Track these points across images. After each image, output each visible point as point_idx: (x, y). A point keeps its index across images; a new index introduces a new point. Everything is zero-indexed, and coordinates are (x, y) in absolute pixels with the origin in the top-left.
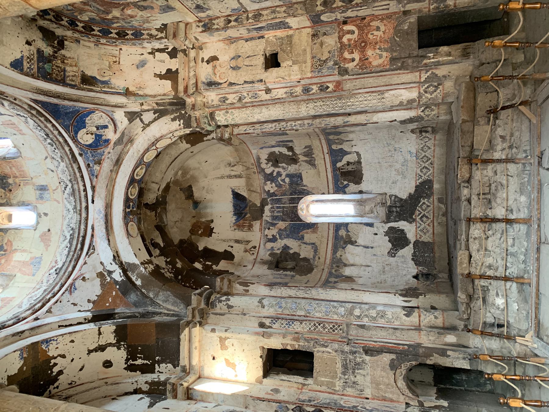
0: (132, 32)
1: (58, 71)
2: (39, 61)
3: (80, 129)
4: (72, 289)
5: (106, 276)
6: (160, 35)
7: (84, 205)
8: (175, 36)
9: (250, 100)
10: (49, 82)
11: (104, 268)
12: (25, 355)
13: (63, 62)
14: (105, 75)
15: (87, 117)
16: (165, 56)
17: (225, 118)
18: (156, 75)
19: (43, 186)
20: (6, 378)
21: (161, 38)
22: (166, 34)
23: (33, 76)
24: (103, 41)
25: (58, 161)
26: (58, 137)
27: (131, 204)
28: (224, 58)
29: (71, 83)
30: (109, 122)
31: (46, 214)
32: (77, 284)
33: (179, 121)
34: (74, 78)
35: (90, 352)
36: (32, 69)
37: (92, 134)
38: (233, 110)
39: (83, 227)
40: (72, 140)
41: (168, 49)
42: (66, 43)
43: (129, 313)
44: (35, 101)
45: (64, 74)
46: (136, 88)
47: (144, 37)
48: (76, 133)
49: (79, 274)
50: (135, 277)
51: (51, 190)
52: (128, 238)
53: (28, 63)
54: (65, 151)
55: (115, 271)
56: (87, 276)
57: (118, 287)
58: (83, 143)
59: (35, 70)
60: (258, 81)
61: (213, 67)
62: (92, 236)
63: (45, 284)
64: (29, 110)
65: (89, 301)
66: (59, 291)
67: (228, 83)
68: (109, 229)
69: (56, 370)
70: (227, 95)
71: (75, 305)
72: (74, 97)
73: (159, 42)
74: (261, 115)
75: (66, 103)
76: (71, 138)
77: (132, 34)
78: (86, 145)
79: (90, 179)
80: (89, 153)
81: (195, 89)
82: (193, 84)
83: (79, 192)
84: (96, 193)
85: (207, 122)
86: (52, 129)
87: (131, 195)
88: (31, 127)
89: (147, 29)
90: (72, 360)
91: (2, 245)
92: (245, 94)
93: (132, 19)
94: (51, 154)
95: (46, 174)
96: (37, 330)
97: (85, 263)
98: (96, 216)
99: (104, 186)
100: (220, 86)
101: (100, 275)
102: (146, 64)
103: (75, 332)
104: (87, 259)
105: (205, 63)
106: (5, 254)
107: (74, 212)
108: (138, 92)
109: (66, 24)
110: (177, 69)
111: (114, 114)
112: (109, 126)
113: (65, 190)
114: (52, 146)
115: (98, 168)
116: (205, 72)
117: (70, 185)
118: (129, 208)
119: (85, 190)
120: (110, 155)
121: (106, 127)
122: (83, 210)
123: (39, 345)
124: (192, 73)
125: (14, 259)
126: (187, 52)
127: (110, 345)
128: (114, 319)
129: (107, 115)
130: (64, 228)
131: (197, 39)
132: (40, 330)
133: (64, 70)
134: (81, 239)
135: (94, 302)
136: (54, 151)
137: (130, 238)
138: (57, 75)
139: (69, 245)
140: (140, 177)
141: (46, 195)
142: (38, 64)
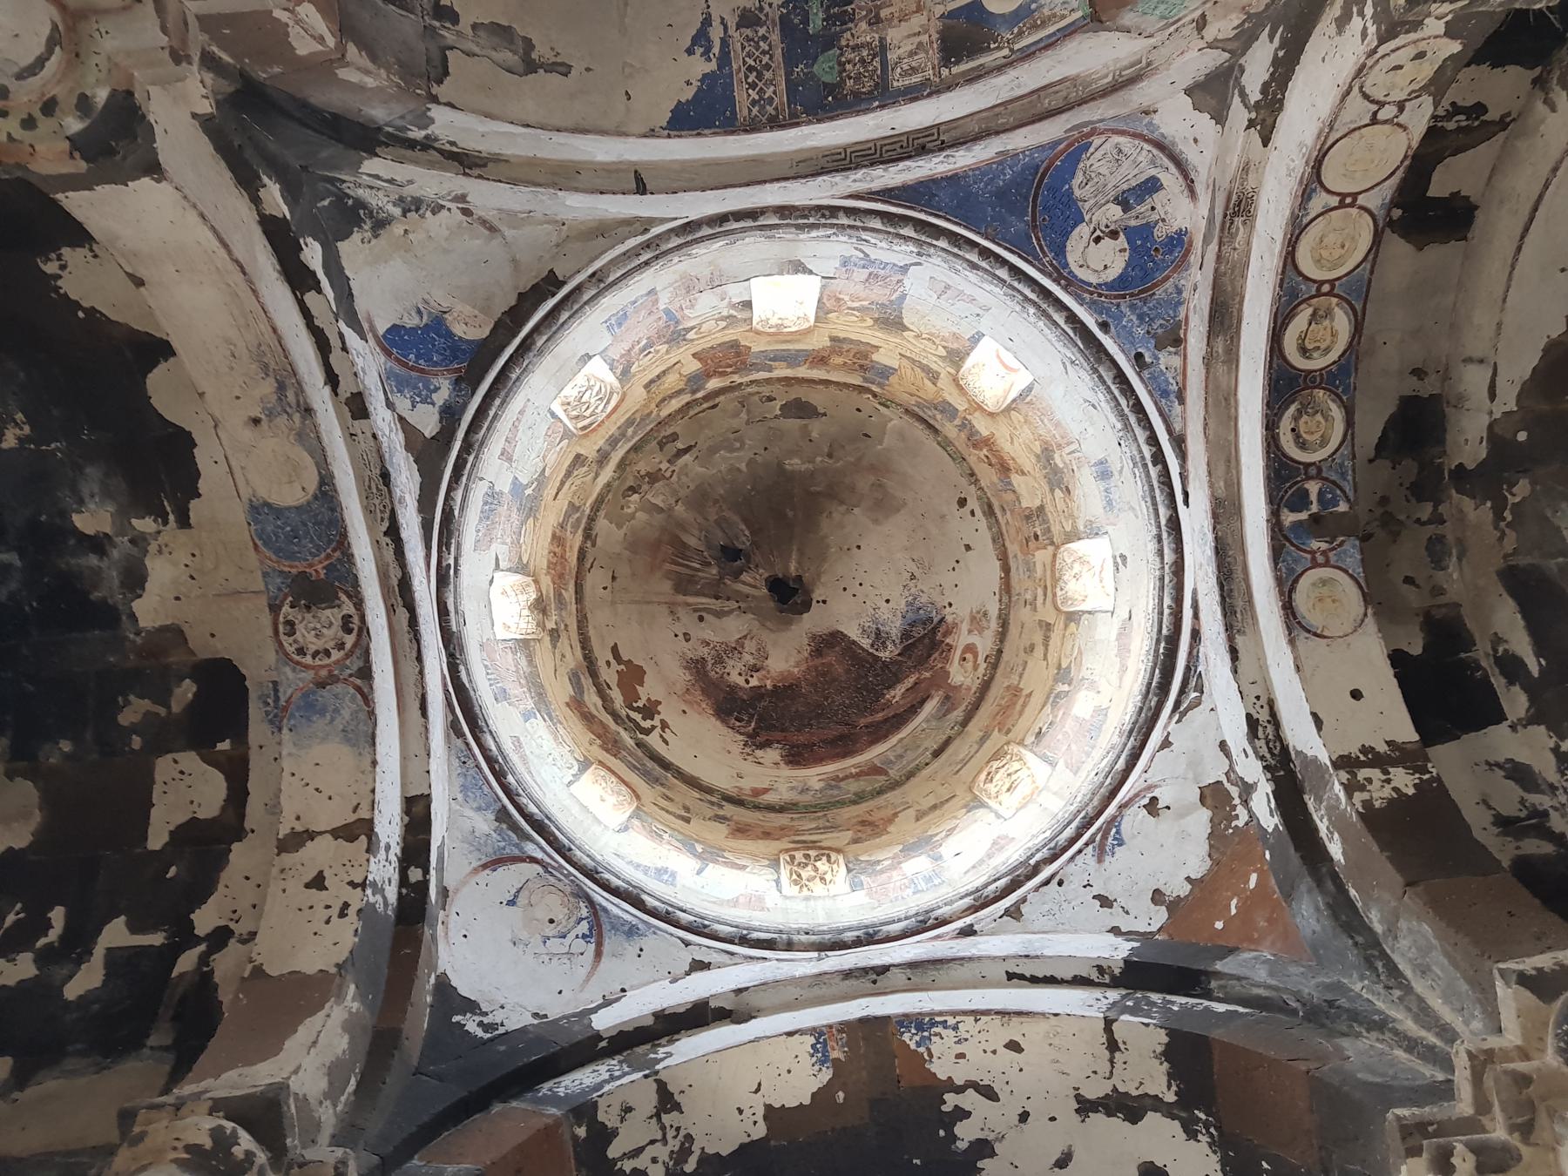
2: (790, 60)
3: (1066, 235)
5: (1237, 801)
10: (832, 119)
11: (1231, 768)
12: (835, 1054)
13: (875, 21)
20: (761, 1111)
23: (775, 123)
27: (1313, 488)
29: (907, 82)
30: (1153, 163)
32: (1126, 826)
35: (1085, 1107)
37: (1114, 235)
39: (1167, 601)
43: (1258, 986)
44: (886, 194)
45: (884, 63)
48: (1060, 251)
49: (1141, 785)
52: (1292, 642)
53: (753, 86)
56: (1165, 796)
58: (1093, 279)
62: (1196, 635)
65: (1157, 897)
68: (1239, 604)
69: (966, 1133)
71: (1105, 902)
76: (1049, 275)
78: (1110, 286)
79: (1161, 414)
87: (1302, 445)
90: (1024, 1117)
96: (932, 974)
101: (1214, 796)
103: (1019, 1013)
112: (1165, 178)
115: (1176, 361)
118: (1301, 501)
119: (1159, 458)
121: (1152, 186)
123: (891, 1029)
127: (1156, 1103)
128: (1208, 995)
129: (1135, 136)
132: (941, 975)
133: (883, 48)
135: (1174, 906)
137: (1306, 643)
138: (858, 77)
140: (1333, 356)
142: (788, 74)
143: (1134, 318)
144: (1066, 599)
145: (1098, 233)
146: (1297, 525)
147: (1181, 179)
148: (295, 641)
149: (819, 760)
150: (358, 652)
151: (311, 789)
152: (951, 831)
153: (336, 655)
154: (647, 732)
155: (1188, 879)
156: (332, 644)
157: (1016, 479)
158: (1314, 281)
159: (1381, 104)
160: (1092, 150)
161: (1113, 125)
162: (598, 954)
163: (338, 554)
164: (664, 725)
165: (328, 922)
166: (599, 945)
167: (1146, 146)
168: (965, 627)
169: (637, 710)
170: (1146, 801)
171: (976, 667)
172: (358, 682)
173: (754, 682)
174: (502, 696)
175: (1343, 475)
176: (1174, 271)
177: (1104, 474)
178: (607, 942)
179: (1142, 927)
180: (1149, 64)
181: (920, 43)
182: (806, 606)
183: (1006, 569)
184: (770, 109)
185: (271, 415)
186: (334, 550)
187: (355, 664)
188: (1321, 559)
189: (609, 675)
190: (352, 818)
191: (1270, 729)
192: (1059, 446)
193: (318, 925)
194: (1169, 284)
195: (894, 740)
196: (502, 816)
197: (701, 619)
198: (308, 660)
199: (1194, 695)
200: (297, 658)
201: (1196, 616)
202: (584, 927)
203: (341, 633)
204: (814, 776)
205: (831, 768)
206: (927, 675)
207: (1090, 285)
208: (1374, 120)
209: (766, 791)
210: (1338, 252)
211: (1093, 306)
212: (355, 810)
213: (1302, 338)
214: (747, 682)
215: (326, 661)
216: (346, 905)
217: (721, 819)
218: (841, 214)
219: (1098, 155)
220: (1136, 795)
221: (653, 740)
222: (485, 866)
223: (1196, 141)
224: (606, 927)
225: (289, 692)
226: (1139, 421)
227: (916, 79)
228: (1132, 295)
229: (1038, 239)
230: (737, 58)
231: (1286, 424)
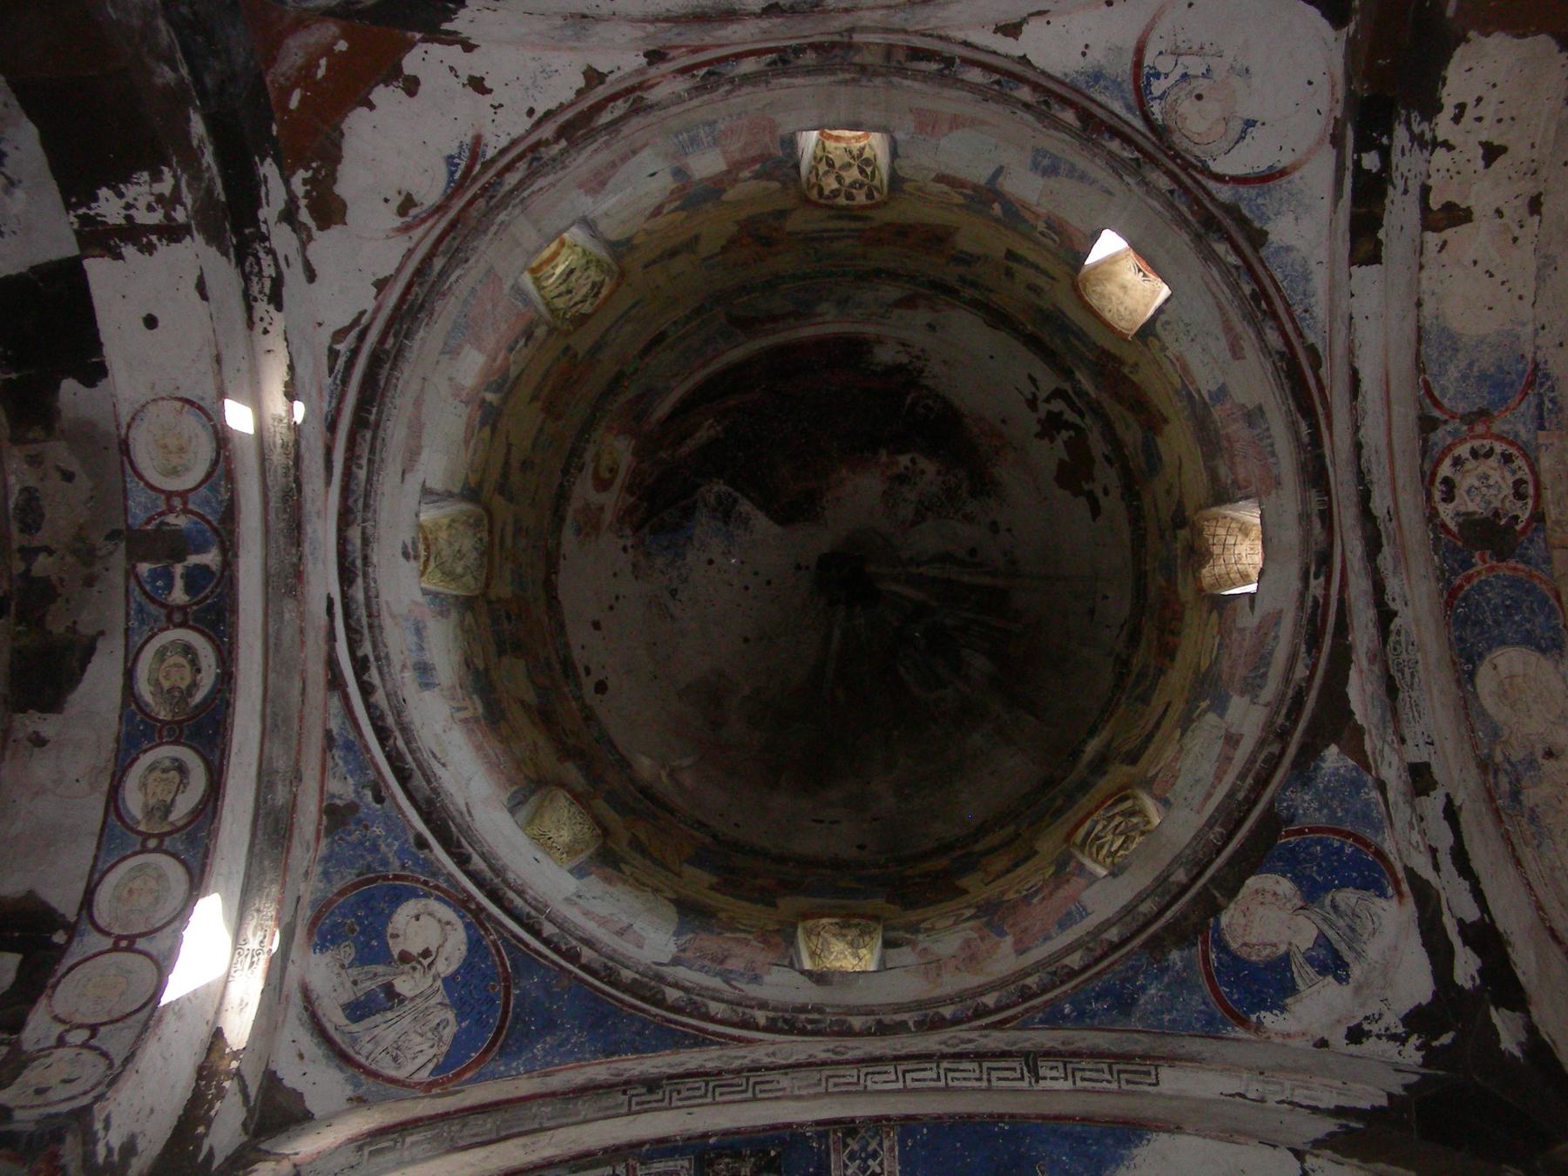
3: (468, 966)
5: (303, 203)
10: (774, 1127)
11: (304, 246)
15: (456, 1037)
23: (849, 1127)
27: (179, 595)
30: (354, 1040)
36: (852, 1157)
37: (405, 957)
48: (475, 945)
49: (418, 233)
65: (412, 86)
71: (477, 85)
72: (584, 1108)
75: (599, 1071)
76: (490, 917)
78: (414, 894)
87: (188, 650)
101: (329, 211)
104: (370, 305)
111: (349, 1091)
115: (334, 786)
118: (197, 577)
119: (360, 666)
121: (358, 1010)
129: (375, 1075)
135: (393, 74)
140: (146, 760)
144: (476, 525)
145: (426, 962)
146: (201, 549)
147: (320, 1013)
148: (1514, 472)
149: (821, 343)
150: (1436, 452)
151: (1499, 277)
152: (657, 211)
154: (1058, 394)
156: (1468, 466)
157: (531, 697)
158: (167, 852)
159: (84, 1045)
160: (431, 1066)
162: (1140, 51)
163: (1457, 581)
164: (1032, 403)
165: (1479, 100)
166: (1138, 64)
167: (362, 1060)
168: (608, 516)
169: (1069, 426)
170: (413, 212)
171: (597, 457)
172: (1436, 413)
173: (904, 460)
174: (1253, 416)
175: (141, 610)
176: (330, 902)
177: (424, 669)
178: (1128, 66)
179: (437, 50)
180: (360, 1148)
182: (825, 562)
183: (550, 586)
184: (854, 1145)
185: (1531, 763)
186: (1461, 587)
187: (1440, 436)
188: (177, 502)
189: (1106, 476)
190: (1448, 233)
191: (255, 289)
193: (1492, 97)
194: (338, 885)
195: (715, 366)
196: (1258, 238)
197: (973, 552)
198: (1499, 447)
199: (341, 347)
201: (329, 451)
202: (1158, 87)
203: (1457, 478)
204: (829, 323)
205: (807, 332)
206: (663, 455)
207: (438, 898)
208: (94, 1029)
209: (899, 304)
210: (138, 884)
211: (434, 870)
212: (1445, 243)
214: (913, 461)
215: (1476, 443)
216: (1457, 119)
217: (966, 259)
219: (421, 1060)
220: (423, 221)
221: (1048, 381)
222: (1283, 173)
223: (301, 1056)
224: (1129, 86)
225: (1524, 405)
226: (382, 717)
228: (386, 878)
229: (503, 964)
231: (207, 679)
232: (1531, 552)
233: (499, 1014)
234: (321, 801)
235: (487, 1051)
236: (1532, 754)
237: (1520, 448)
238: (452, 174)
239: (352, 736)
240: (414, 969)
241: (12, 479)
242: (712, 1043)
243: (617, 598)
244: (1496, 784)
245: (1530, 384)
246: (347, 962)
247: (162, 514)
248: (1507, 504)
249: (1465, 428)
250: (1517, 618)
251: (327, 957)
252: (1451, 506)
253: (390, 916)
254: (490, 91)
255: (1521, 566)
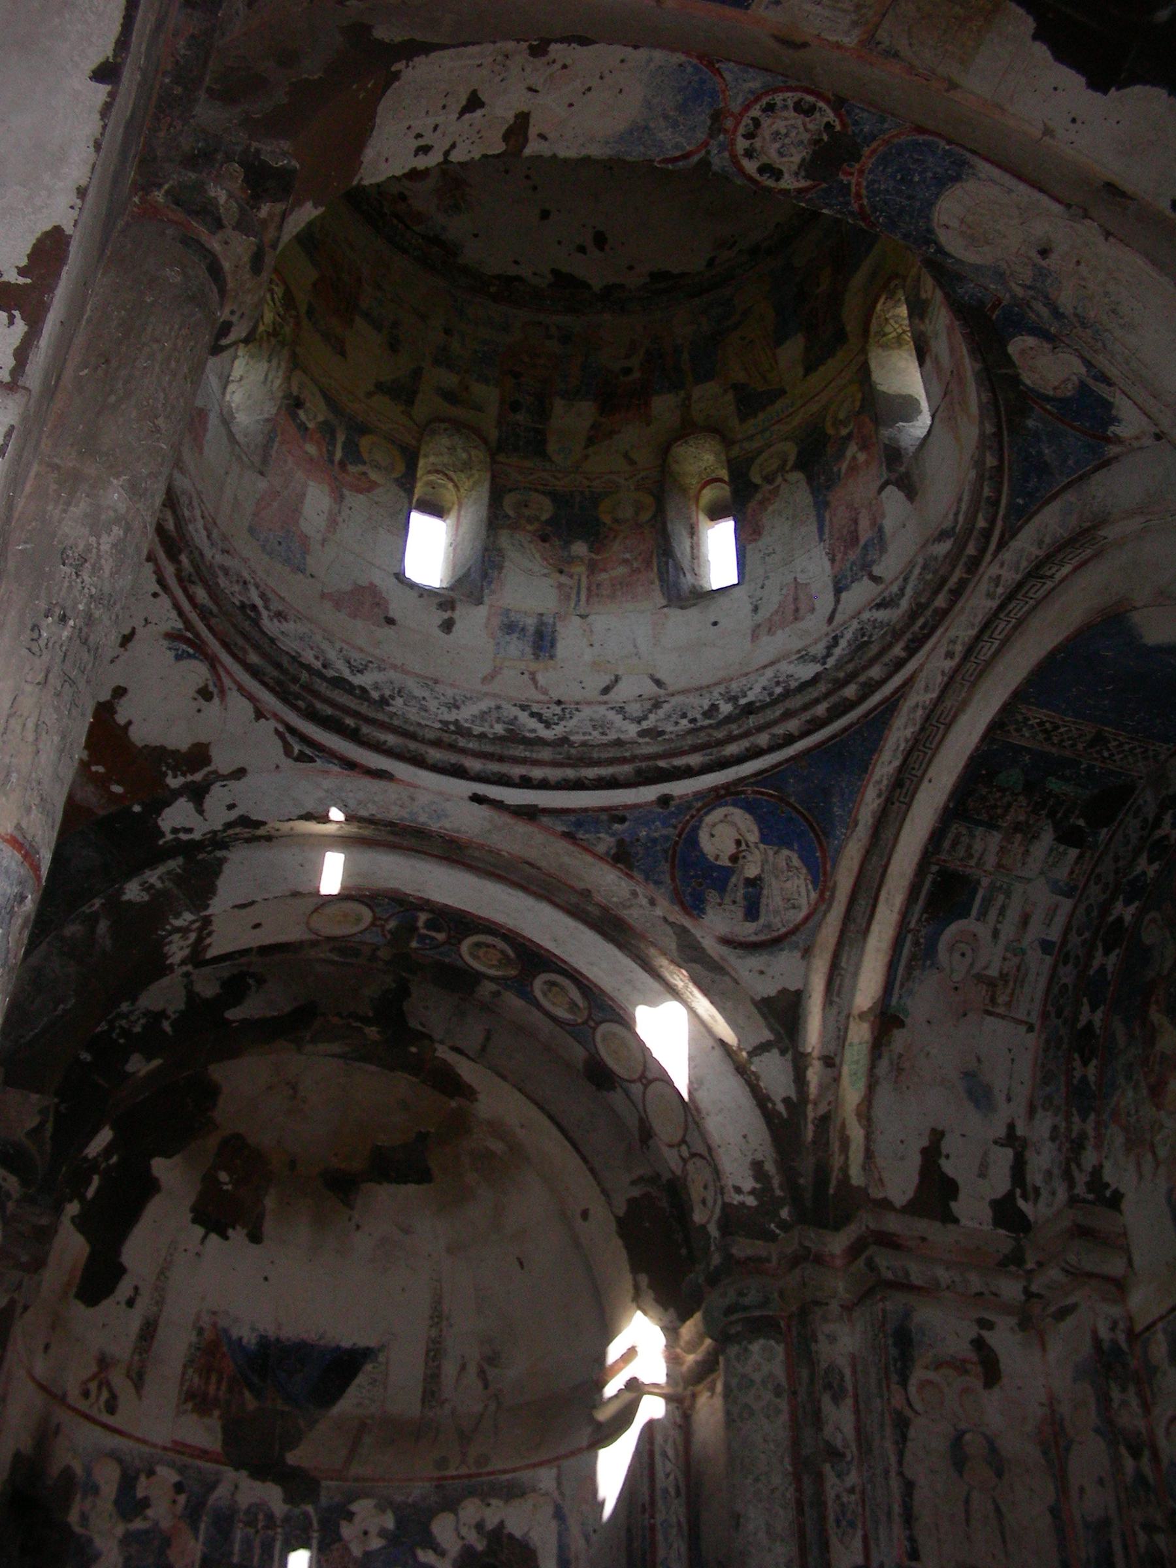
0: (1092, 1079)
1: (995, 807)
3: (760, 820)
4: (185, 642)
5: (190, 778)
6: (1081, 1179)
7: (474, 765)
8: (1082, 1232)
9: (831, 1494)
13: (1017, 828)
14: (957, 955)
15: (801, 858)
16: (999, 1183)
17: (757, 1377)
18: (937, 1136)
19: (553, 644)
21: (1071, 1184)
22: (1084, 1201)
23: (996, 727)
24: (1067, 975)
25: (645, 718)
26: (745, 744)
27: (441, 937)
28: (992, 1410)
29: (950, 836)
30: (768, 926)
31: (448, 626)
33: (753, 1192)
34: (961, 852)
37: (734, 858)
38: (784, 1417)
39: (391, 739)
40: (726, 786)
41: (1025, 1197)
42: (1073, 853)
44: (891, 706)
45: (979, 823)
46: (900, 1056)
47: (1076, 1119)
48: (749, 807)
49: (227, 682)
50: (159, 885)
51: (533, 666)
53: (1041, 724)
54: (683, 753)
55: (200, 811)
57: (137, 809)
58: (709, 819)
59: (1015, 739)
60: (912, 1539)
61: (964, 1361)
62: (351, 765)
63: (219, 558)
64: (862, 678)
66: (191, 599)
67: (908, 1413)
70: (849, 1401)
73: (1056, 1171)
74: (762, 1535)
75: (870, 802)
77: (1084, 1079)
78: (696, 829)
80: (665, 832)
81: (889, 1275)
82: (907, 1274)
83: (524, 761)
84: (506, 819)
85: (746, 1301)
86: (779, 730)
87: (478, 945)
88: (785, 668)
89: (1099, 1137)
91: (364, 463)
92: (852, 1478)
93: (1145, 1092)
94: (674, 701)
95: (595, 666)
97: (259, 715)
98: (423, 798)
99: (532, 854)
100: (895, 1378)
101: (199, 756)
102: (977, 1105)
104: (273, 723)
105: (973, 1332)
106: (332, 461)
107: (446, 723)
108: (886, 1056)
109: (1139, 870)
110: (956, 1221)
113: (532, 715)
114: (706, 714)
115: (601, 848)
116: (945, 1328)
117: (547, 734)
118: (432, 925)
119: (526, 783)
120: (644, 902)
121: (752, 912)
122: (453, 758)
124: (943, 1275)
125: (311, 483)
126: (1013, 1268)
130: (392, 674)
131: (1063, 1313)
133: (991, 825)
134: (350, 722)
136: (684, 716)
139: (330, 673)
141: (516, 647)
142: (1029, 751)
143: (656, 835)
145: (744, 847)
146: (416, 919)
147: (742, 939)
148: (786, 107)
153: (741, 144)
155: (130, 723)
158: (601, 1022)
160: (810, 886)
161: (816, 918)
163: (855, 207)
167: (783, 930)
170: (211, 688)
172: (695, 159)
176: (675, 889)
181: (971, 856)
186: (861, 207)
190: (533, 132)
192: (593, 568)
198: (755, 112)
199: (297, 748)
200: (764, 101)
203: (765, 159)
207: (706, 814)
208: (683, 1141)
212: (542, 136)
213: (563, 988)
215: (741, 130)
218: (903, 654)
220: (219, 678)
223: (762, 972)
225: (726, 75)
227: (946, 844)
228: (677, 843)
230: (1074, 723)
231: (501, 945)
232: (867, 128)
233: (802, 820)
234: (608, 862)
235: (820, 842)
236: (1034, 265)
237: (766, 93)
238: (189, 656)
239: (572, 818)
240: (744, 857)
241: (322, 955)
242: (898, 701)
243: (528, 177)
244: (1038, 315)
245: (710, 65)
246: (719, 901)
247: (383, 930)
248: (810, 126)
249: (721, 137)
250: (916, 179)
251: (709, 910)
252: (786, 176)
253: (703, 855)
254: (134, 629)
255: (874, 145)
